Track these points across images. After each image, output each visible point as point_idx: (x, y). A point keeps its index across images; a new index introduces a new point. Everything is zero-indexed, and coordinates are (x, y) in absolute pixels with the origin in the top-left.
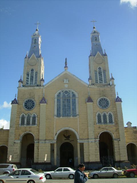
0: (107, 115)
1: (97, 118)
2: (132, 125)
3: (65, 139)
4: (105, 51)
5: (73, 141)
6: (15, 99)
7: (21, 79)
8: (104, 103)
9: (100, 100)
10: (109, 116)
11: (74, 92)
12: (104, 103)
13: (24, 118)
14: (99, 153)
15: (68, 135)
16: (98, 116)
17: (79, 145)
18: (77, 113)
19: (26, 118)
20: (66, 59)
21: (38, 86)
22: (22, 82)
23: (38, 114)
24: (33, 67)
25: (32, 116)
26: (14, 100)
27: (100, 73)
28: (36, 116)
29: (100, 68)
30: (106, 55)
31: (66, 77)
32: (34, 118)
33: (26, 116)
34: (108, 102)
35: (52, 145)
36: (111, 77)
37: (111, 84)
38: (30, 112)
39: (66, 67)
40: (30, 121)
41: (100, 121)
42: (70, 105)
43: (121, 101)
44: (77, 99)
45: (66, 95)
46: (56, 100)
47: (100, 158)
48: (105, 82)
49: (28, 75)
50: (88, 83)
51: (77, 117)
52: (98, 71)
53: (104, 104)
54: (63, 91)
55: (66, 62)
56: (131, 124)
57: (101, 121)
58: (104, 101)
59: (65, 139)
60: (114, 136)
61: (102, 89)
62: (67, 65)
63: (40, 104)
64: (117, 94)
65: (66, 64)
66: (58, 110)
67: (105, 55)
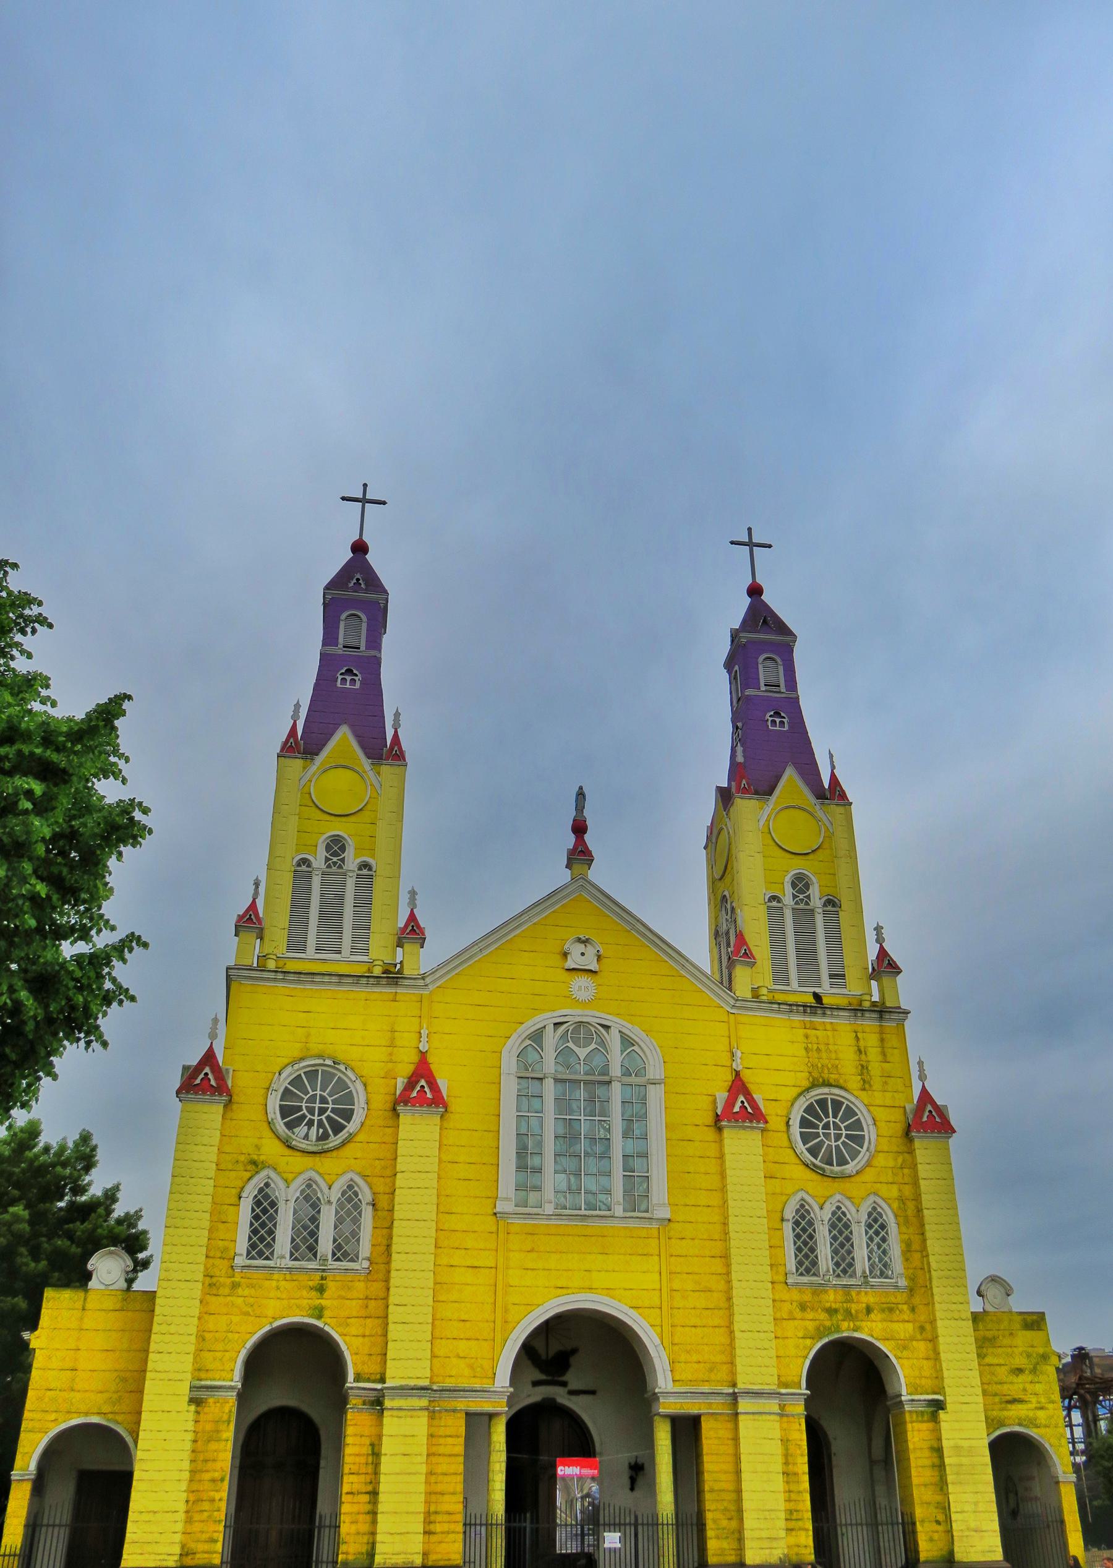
0: (858, 1217)
3: (543, 1377)
5: (593, 1392)
7: (253, 906)
9: (810, 1109)
10: (870, 1226)
15: (551, 1353)
16: (797, 1223)
19: (291, 1204)
20: (581, 795)
23: (381, 1186)
25: (335, 1195)
28: (366, 1195)
30: (843, 796)
34: (858, 1125)
38: (327, 1164)
39: (580, 855)
41: (807, 1261)
42: (609, 1130)
44: (654, 1094)
45: (582, 1053)
52: (788, 900)
53: (838, 1137)
54: (557, 1025)
57: (814, 1263)
58: (835, 1117)
59: (543, 1377)
60: (907, 1377)
62: (587, 837)
63: (394, 1109)
64: (922, 1077)
65: (579, 828)
66: (522, 1153)
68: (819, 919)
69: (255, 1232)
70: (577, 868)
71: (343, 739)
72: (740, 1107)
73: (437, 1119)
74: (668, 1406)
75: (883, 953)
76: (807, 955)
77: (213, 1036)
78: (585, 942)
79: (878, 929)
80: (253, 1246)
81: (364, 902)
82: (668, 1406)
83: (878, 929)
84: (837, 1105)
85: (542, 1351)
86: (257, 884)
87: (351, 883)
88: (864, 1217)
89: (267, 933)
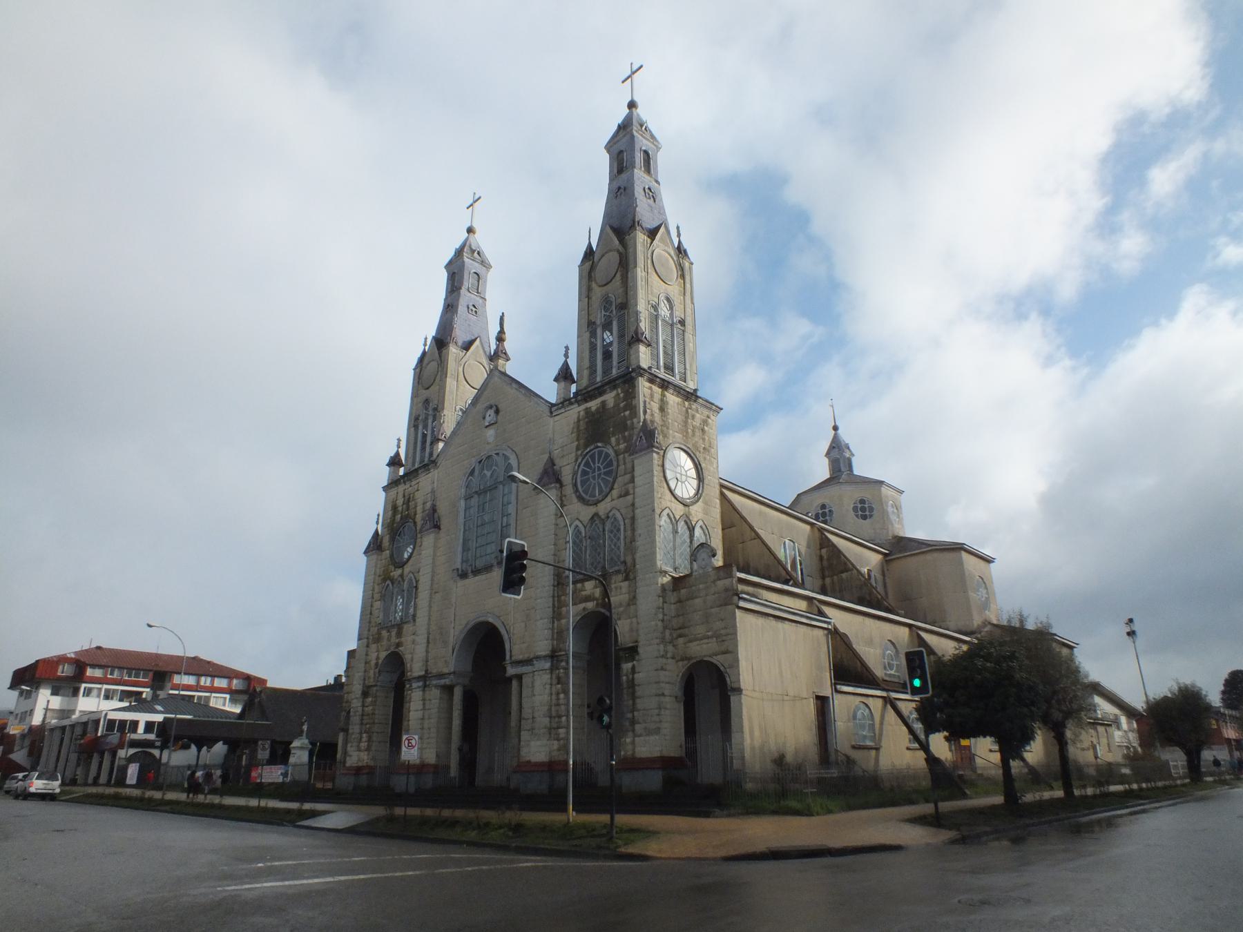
6: (377, 531)
7: (397, 454)
20: (502, 319)
35: (449, 689)
45: (488, 474)
46: (462, 503)
49: (416, 427)
50: (553, 399)
55: (502, 332)
61: (594, 405)
74: (511, 671)
78: (491, 407)
82: (511, 671)
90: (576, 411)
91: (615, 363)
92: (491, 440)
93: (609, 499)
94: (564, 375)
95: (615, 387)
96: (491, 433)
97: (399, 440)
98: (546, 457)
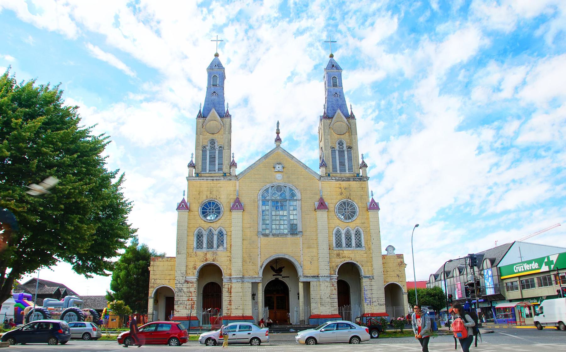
1: (334, 238)
2: (396, 252)
4: (351, 109)
6: (183, 201)
7: (192, 161)
8: (347, 210)
11: (293, 188)
12: (347, 210)
13: (202, 235)
14: (336, 300)
16: (336, 235)
17: (301, 285)
18: (300, 229)
20: (278, 123)
21: (225, 175)
22: (194, 167)
23: (228, 230)
24: (215, 137)
25: (216, 233)
26: (182, 202)
27: (341, 152)
28: (225, 232)
29: (341, 144)
31: (277, 158)
32: (221, 234)
33: (205, 233)
36: (360, 162)
37: (361, 175)
40: (212, 242)
41: (339, 244)
43: (378, 208)
47: (339, 310)
48: (350, 169)
49: (204, 151)
51: (298, 236)
52: (337, 148)
56: (394, 249)
60: (364, 271)
61: (344, 184)
62: (281, 136)
64: (372, 195)
65: (278, 133)
67: (352, 117)
68: (346, 153)
69: (198, 242)
70: (278, 143)
71: (213, 112)
72: (322, 205)
73: (241, 213)
74: (302, 279)
75: (363, 162)
76: (342, 164)
77: (184, 195)
79: (362, 155)
80: (198, 246)
81: (221, 157)
83: (362, 155)
84: (348, 204)
85: (275, 268)
86: (192, 154)
87: (217, 152)
88: (354, 231)
89: (196, 167)
90: (334, 184)
91: (347, 168)
92: (279, 178)
93: (354, 222)
94: (323, 164)
95: (356, 181)
96: (279, 176)
97: (192, 154)
98: (318, 197)
